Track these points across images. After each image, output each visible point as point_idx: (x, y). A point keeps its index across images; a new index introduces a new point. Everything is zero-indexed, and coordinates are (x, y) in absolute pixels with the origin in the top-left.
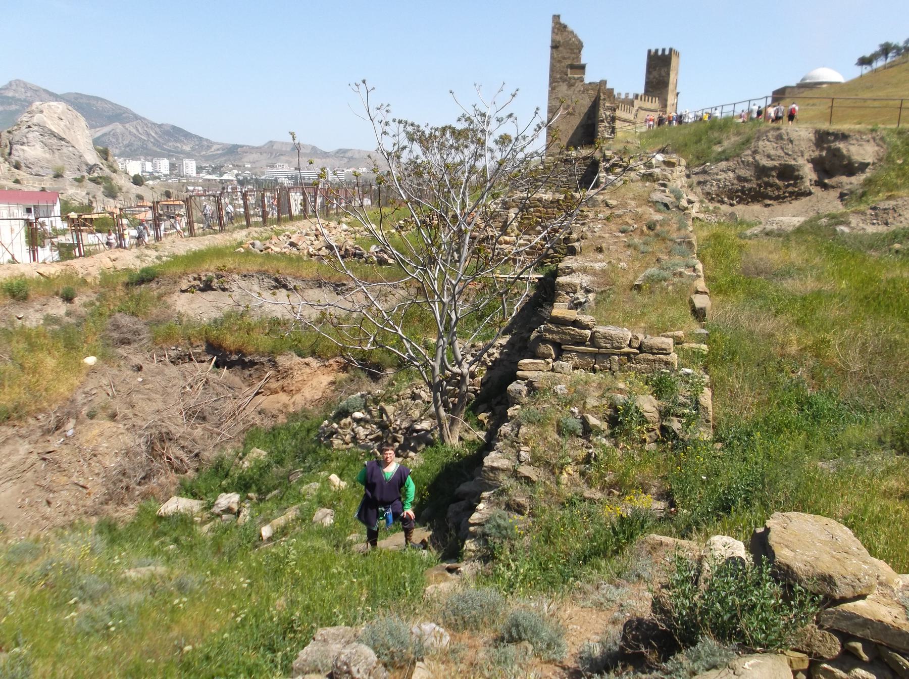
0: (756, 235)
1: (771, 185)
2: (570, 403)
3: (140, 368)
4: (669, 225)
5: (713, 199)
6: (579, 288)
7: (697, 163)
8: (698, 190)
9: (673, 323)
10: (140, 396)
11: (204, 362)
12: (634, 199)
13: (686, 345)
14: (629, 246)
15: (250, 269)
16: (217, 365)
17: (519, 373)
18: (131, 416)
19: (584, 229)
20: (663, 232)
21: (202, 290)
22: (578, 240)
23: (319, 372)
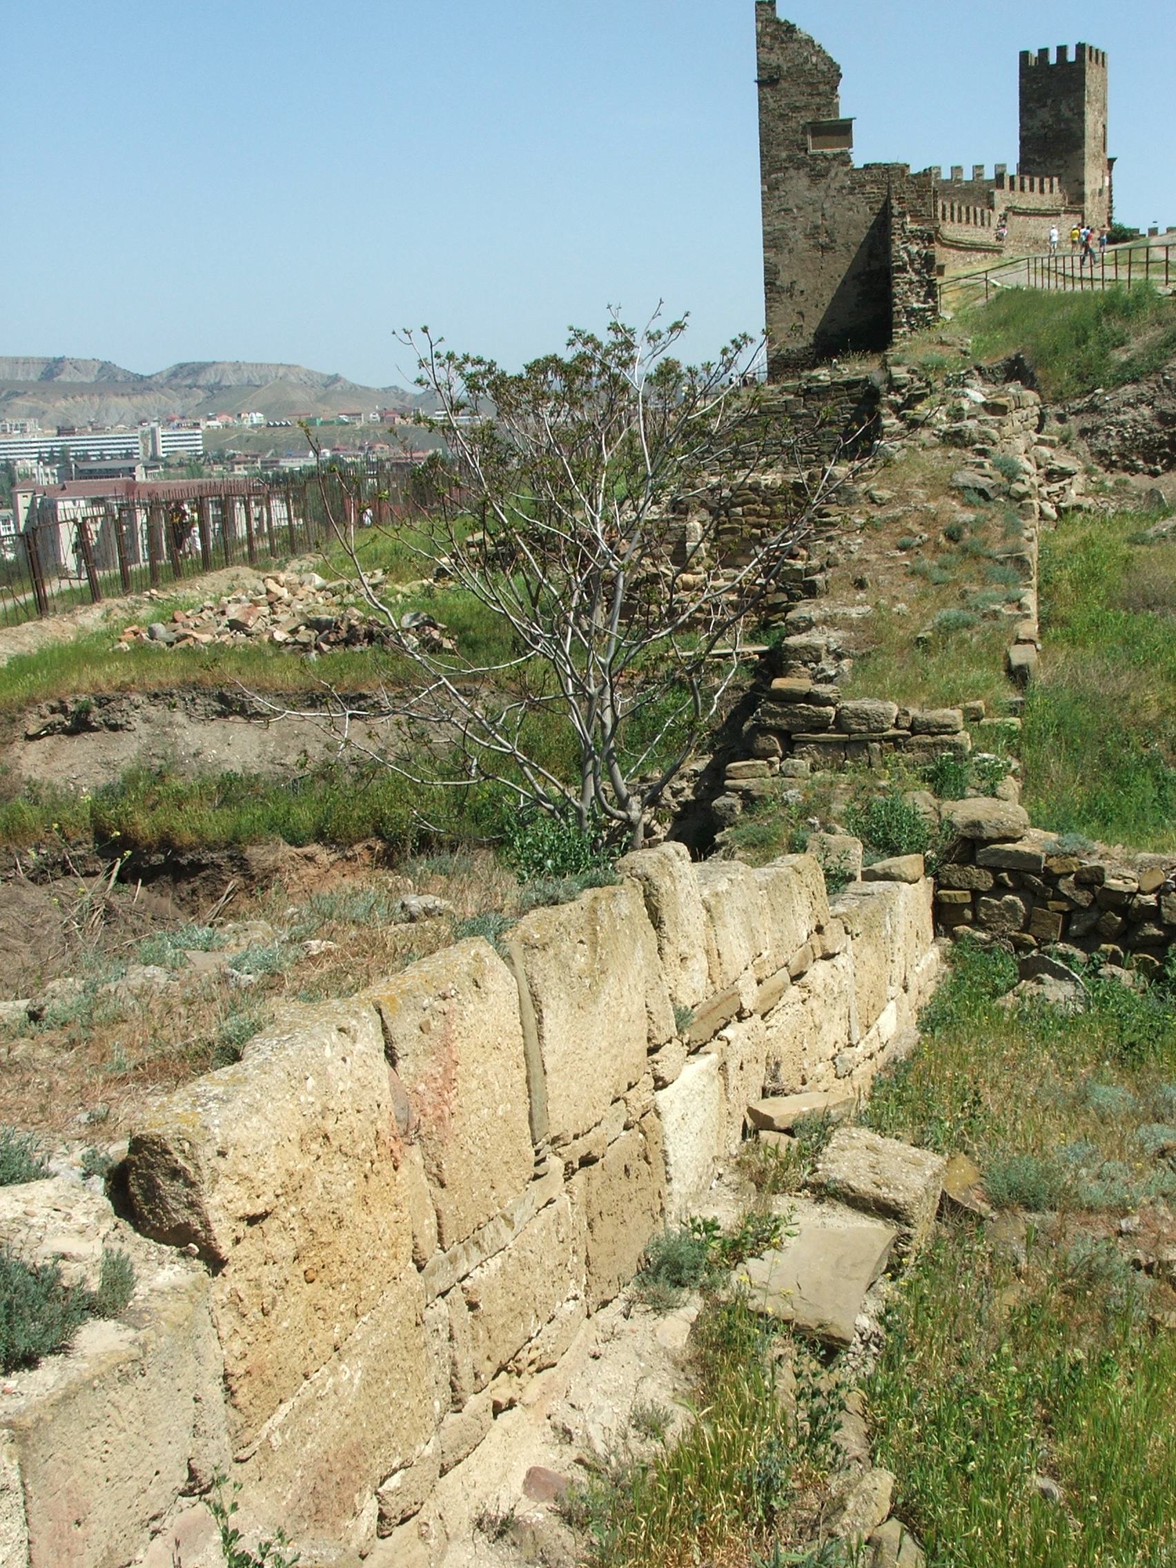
5: (1113, 464)
6: (823, 652)
8: (1082, 446)
11: (95, 874)
12: (922, 485)
13: (985, 721)
14: (913, 573)
15: (164, 680)
16: (121, 879)
17: (727, 782)
19: (832, 549)
20: (974, 544)
21: (71, 732)
22: (822, 570)
23: (333, 871)
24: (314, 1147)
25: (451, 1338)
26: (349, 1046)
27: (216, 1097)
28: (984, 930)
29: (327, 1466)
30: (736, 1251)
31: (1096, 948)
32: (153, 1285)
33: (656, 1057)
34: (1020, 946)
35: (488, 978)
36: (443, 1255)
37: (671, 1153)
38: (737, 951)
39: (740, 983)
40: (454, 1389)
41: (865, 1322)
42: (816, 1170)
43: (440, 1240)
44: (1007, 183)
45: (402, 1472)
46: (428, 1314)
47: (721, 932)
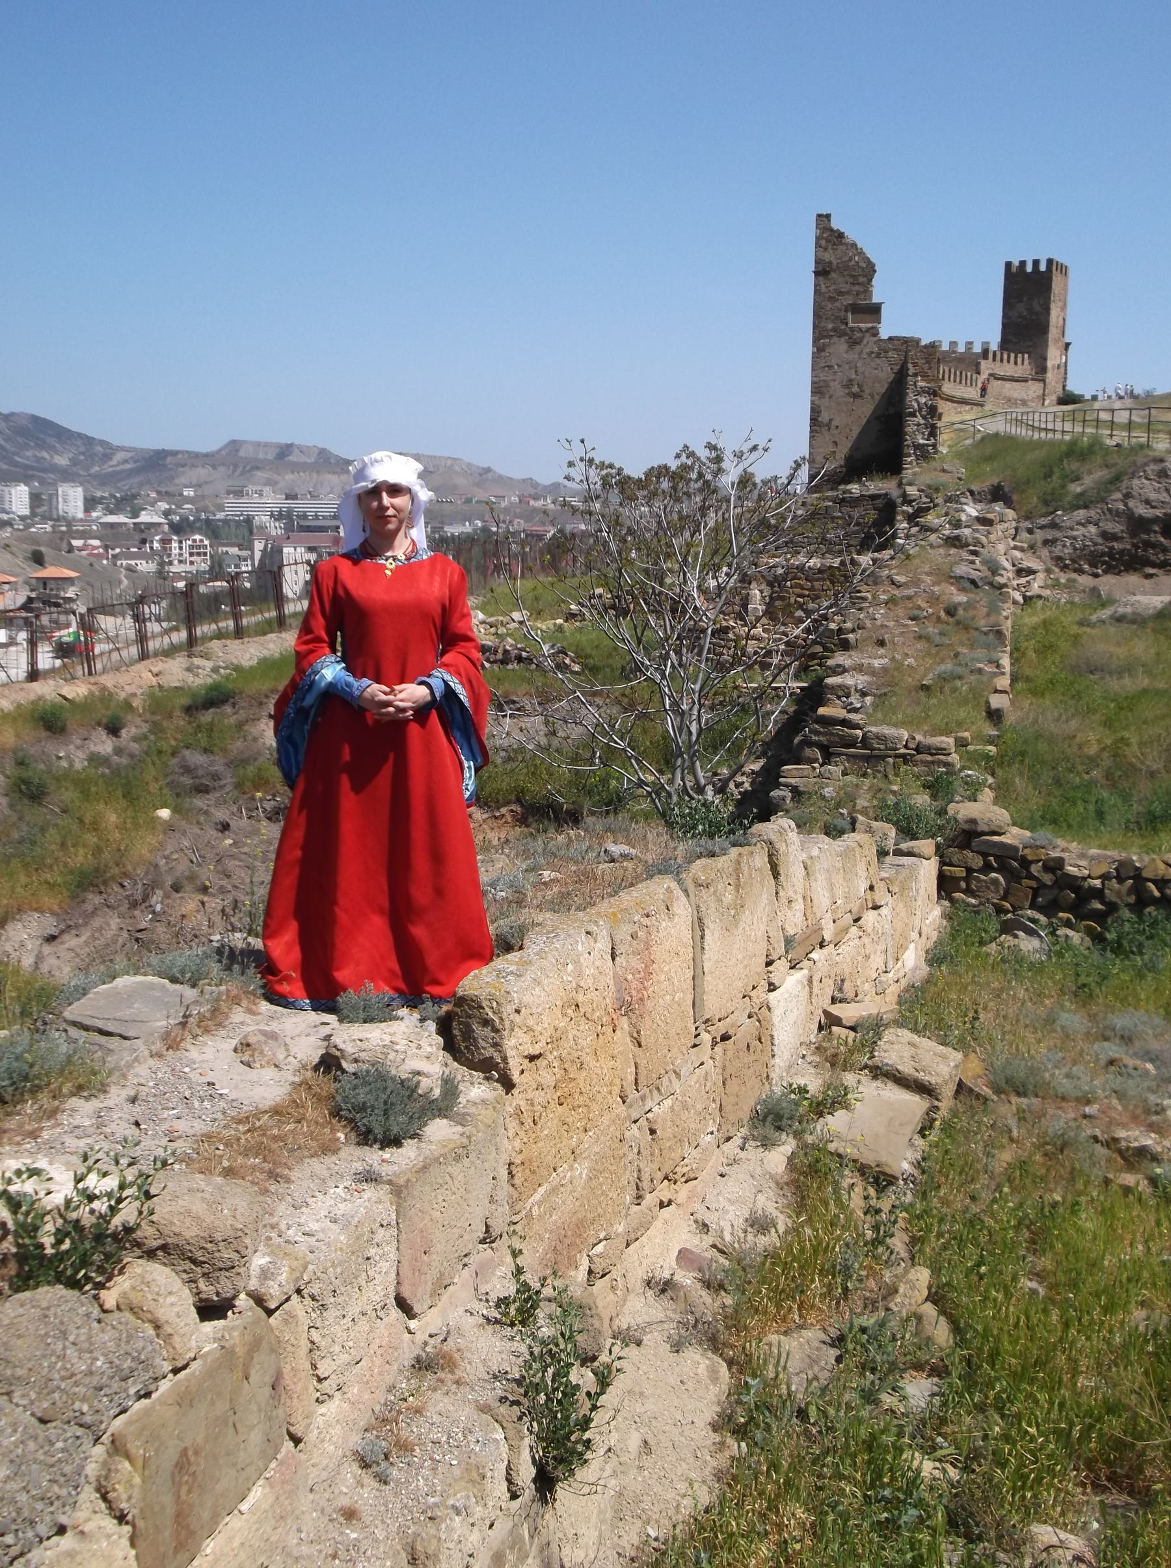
0: (1103, 622)
1: (1153, 546)
2: (838, 805)
3: (225, 827)
4: (975, 608)
6: (853, 690)
7: (1044, 510)
8: (1045, 552)
9: (960, 724)
10: (237, 863)
12: (928, 574)
13: (970, 748)
14: (920, 637)
18: (230, 887)
19: (862, 616)
22: (853, 631)
23: (485, 826)
24: (570, 1011)
25: (639, 1153)
26: (592, 944)
27: (512, 973)
28: (975, 897)
29: (563, 1232)
30: (821, 1108)
31: (1055, 916)
32: (468, 1098)
33: (770, 968)
34: (1000, 910)
35: (675, 905)
36: (637, 1095)
37: (776, 1037)
38: (822, 900)
39: (823, 921)
40: (638, 1189)
41: (906, 1166)
42: (874, 1057)
43: (636, 1083)
44: (991, 355)
45: (604, 1242)
46: (627, 1134)
47: (813, 884)
